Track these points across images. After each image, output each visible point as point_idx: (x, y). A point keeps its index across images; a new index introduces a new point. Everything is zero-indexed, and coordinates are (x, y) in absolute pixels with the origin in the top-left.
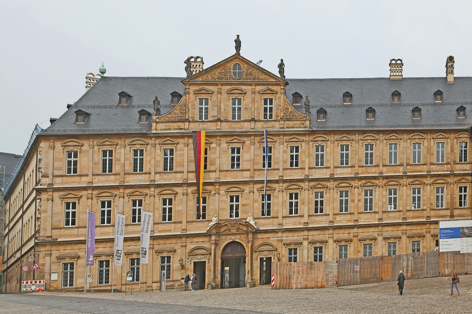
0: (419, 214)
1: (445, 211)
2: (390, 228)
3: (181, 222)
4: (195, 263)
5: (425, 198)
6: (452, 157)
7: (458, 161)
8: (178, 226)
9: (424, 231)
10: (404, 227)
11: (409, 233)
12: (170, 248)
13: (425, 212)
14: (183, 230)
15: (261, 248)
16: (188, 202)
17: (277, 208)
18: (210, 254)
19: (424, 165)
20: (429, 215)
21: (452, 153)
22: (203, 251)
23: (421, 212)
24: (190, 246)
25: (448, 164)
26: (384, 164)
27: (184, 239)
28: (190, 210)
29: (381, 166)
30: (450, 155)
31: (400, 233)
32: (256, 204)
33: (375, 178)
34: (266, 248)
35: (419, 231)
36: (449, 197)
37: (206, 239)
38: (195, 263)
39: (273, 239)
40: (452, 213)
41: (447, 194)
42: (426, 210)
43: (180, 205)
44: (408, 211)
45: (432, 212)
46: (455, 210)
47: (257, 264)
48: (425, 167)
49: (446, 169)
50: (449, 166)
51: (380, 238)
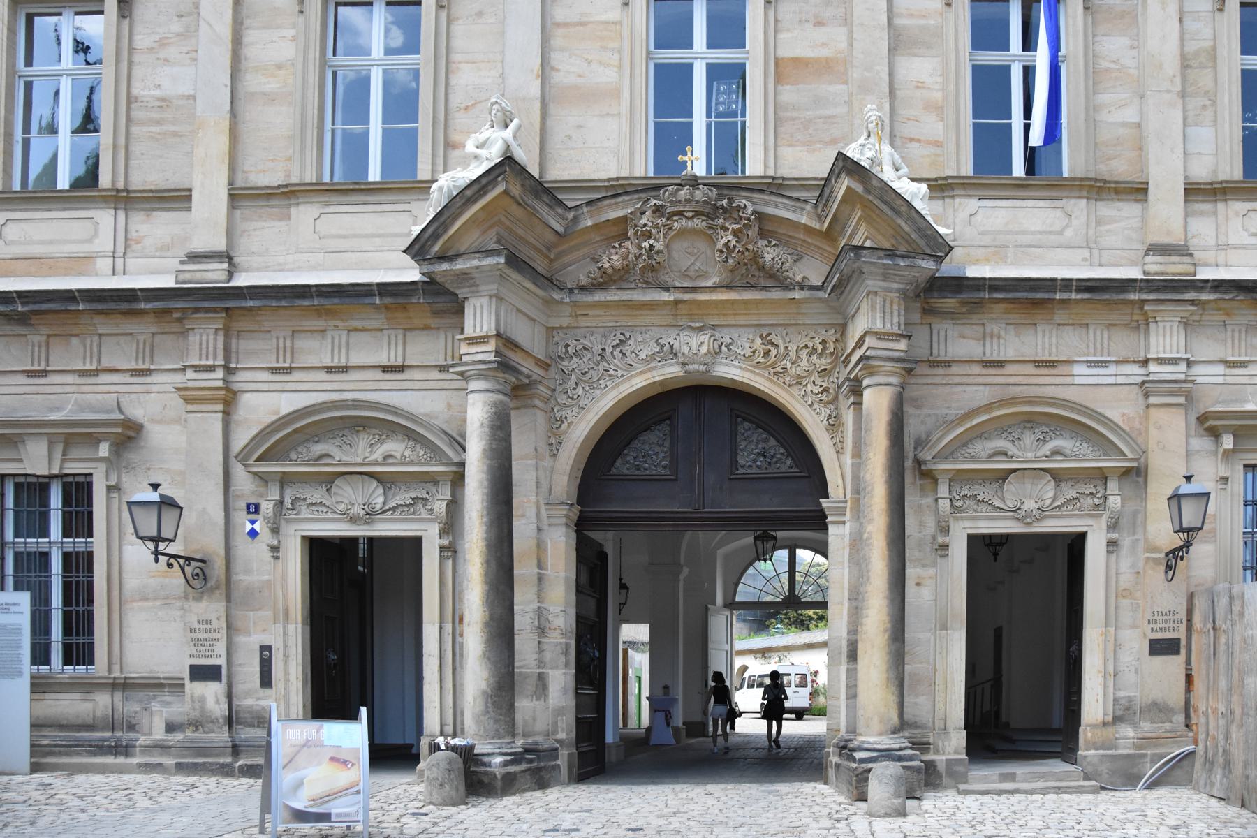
3: (178, 198)
4: (318, 549)
8: (156, 228)
12: (81, 408)
14: (194, 257)
15: (984, 447)
16: (250, 37)
17: (1130, 115)
18: (458, 478)
22: (395, 447)
24: (266, 403)
27: (204, 339)
28: (270, 98)
32: (919, 70)
34: (1028, 450)
37: (425, 349)
38: (318, 549)
39: (1095, 372)
43: (172, 52)
47: (944, 587)
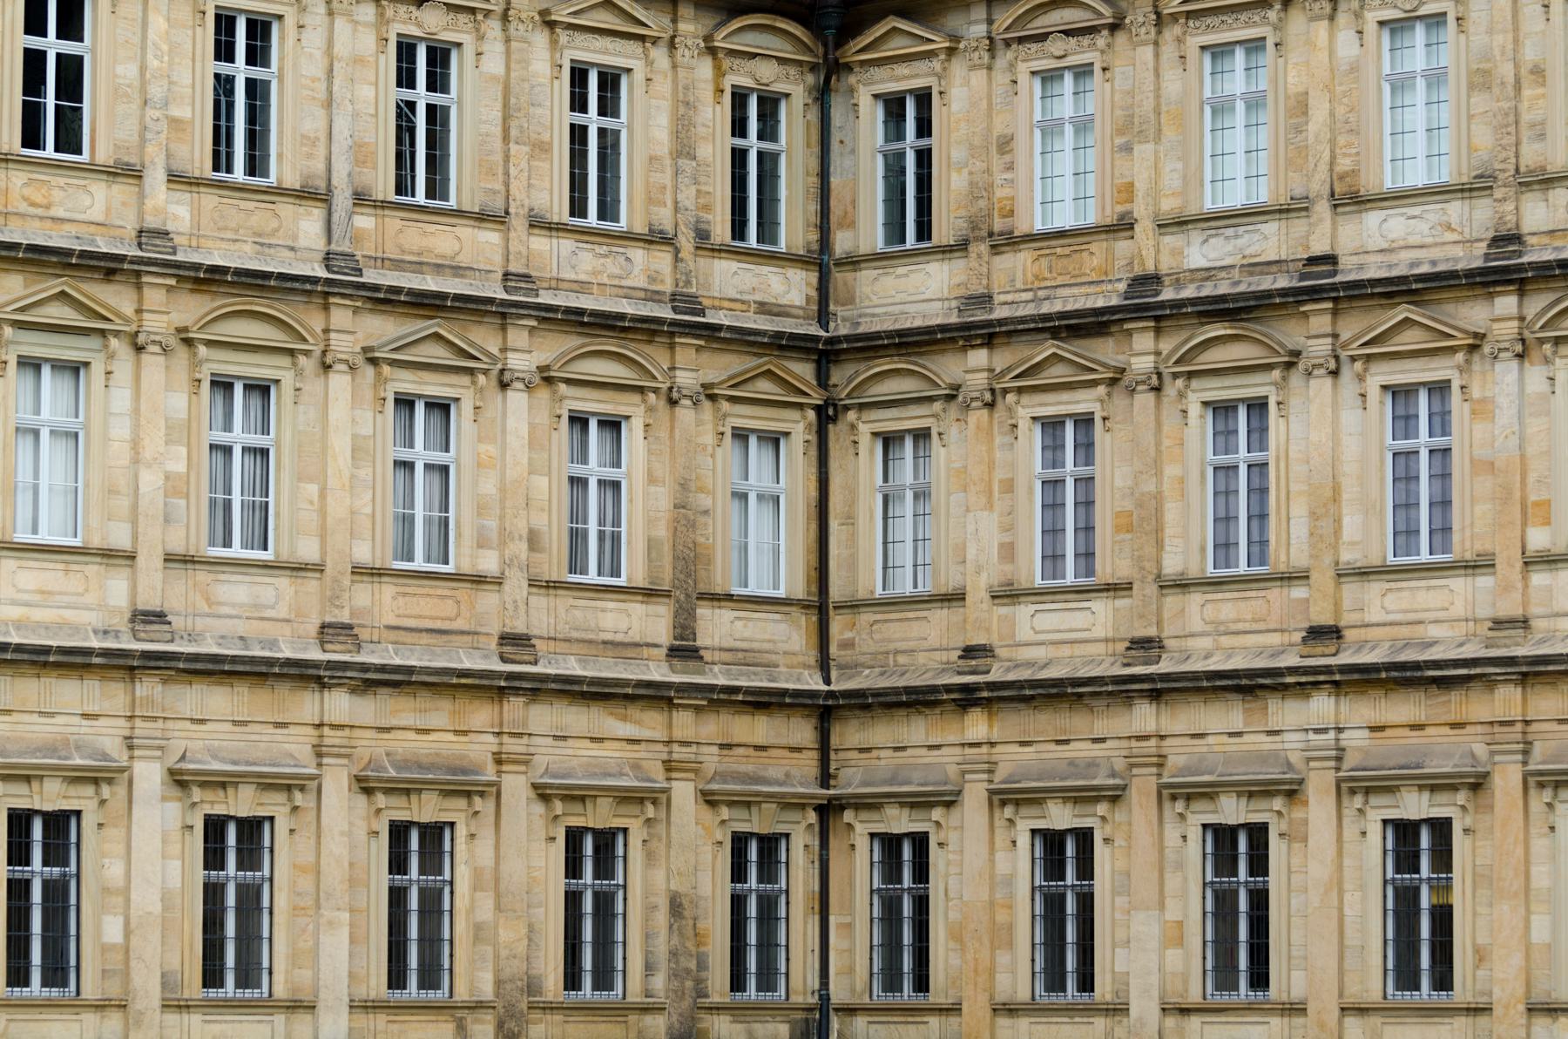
0: (448, 608)
1: (637, 609)
2: (217, 700)
5: (489, 487)
6: (687, 196)
7: (721, 230)
9: (480, 749)
10: (340, 704)
11: (369, 746)
13: (488, 600)
19: (482, 218)
20: (520, 627)
21: (684, 163)
23: (463, 591)
25: (656, 238)
26: (179, 166)
29: (156, 177)
30: (666, 178)
31: (292, 752)
33: (108, 267)
35: (443, 745)
36: (663, 498)
40: (684, 627)
41: (652, 479)
42: (498, 582)
44: (358, 571)
45: (540, 601)
46: (704, 611)
48: (490, 237)
49: (641, 282)
50: (662, 260)
51: (149, 775)
